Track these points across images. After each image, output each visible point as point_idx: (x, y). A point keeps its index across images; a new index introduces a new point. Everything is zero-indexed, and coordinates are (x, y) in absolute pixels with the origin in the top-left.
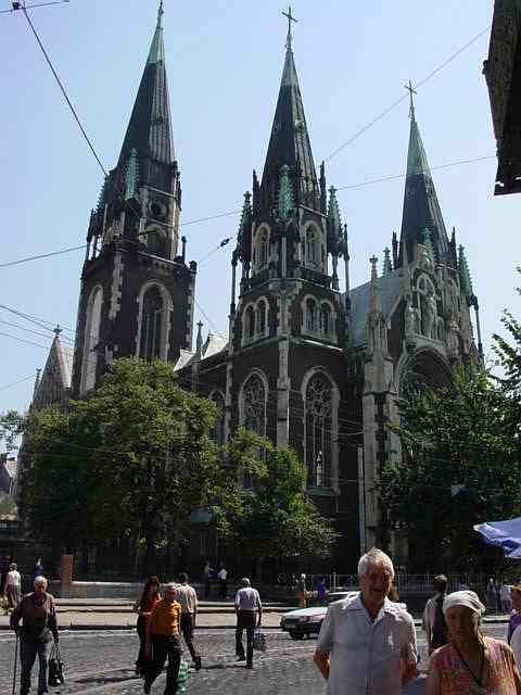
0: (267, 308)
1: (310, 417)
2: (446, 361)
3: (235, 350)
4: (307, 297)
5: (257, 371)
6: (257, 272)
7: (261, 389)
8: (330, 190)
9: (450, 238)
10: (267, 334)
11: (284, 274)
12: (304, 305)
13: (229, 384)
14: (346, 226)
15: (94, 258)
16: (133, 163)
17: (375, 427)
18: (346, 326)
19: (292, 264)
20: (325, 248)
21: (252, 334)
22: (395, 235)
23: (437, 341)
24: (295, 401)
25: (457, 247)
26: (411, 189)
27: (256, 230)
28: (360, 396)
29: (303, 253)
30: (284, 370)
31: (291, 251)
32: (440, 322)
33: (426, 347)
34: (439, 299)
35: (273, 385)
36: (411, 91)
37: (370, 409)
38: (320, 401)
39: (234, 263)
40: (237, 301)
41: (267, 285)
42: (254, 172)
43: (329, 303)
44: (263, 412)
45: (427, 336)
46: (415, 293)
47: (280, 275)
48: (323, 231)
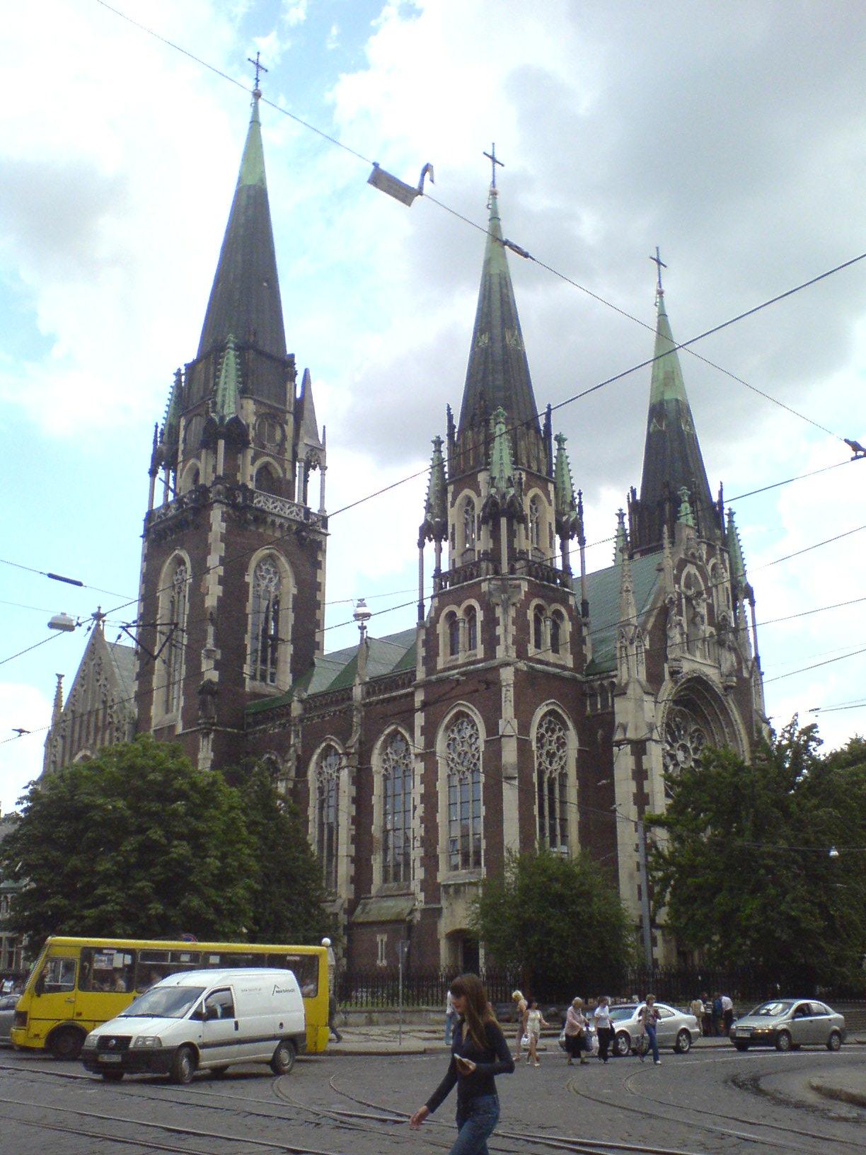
0: (480, 616)
1: (541, 774)
2: (719, 689)
3: (429, 672)
4: (535, 602)
5: (465, 706)
6: (458, 565)
7: (468, 732)
8: (556, 439)
9: (715, 498)
10: (480, 652)
11: (505, 568)
12: (530, 615)
13: (419, 719)
14: (580, 494)
15: (167, 505)
16: (231, 358)
17: (632, 787)
18: (583, 642)
19: (515, 556)
20: (554, 529)
21: (453, 651)
22: (633, 492)
23: (709, 662)
24: (523, 747)
25: (726, 511)
26: (660, 422)
27: (454, 499)
28: (609, 744)
29: (527, 538)
30: (508, 710)
31: (512, 534)
32: (711, 632)
33: (694, 671)
34: (710, 601)
35: (492, 728)
36: (659, 263)
37: (624, 762)
38: (554, 746)
39: (421, 545)
40: (428, 604)
41: (480, 582)
42: (449, 409)
43: (563, 611)
44: (475, 765)
45: (695, 656)
46: (679, 594)
47: (497, 572)
48: (550, 505)
